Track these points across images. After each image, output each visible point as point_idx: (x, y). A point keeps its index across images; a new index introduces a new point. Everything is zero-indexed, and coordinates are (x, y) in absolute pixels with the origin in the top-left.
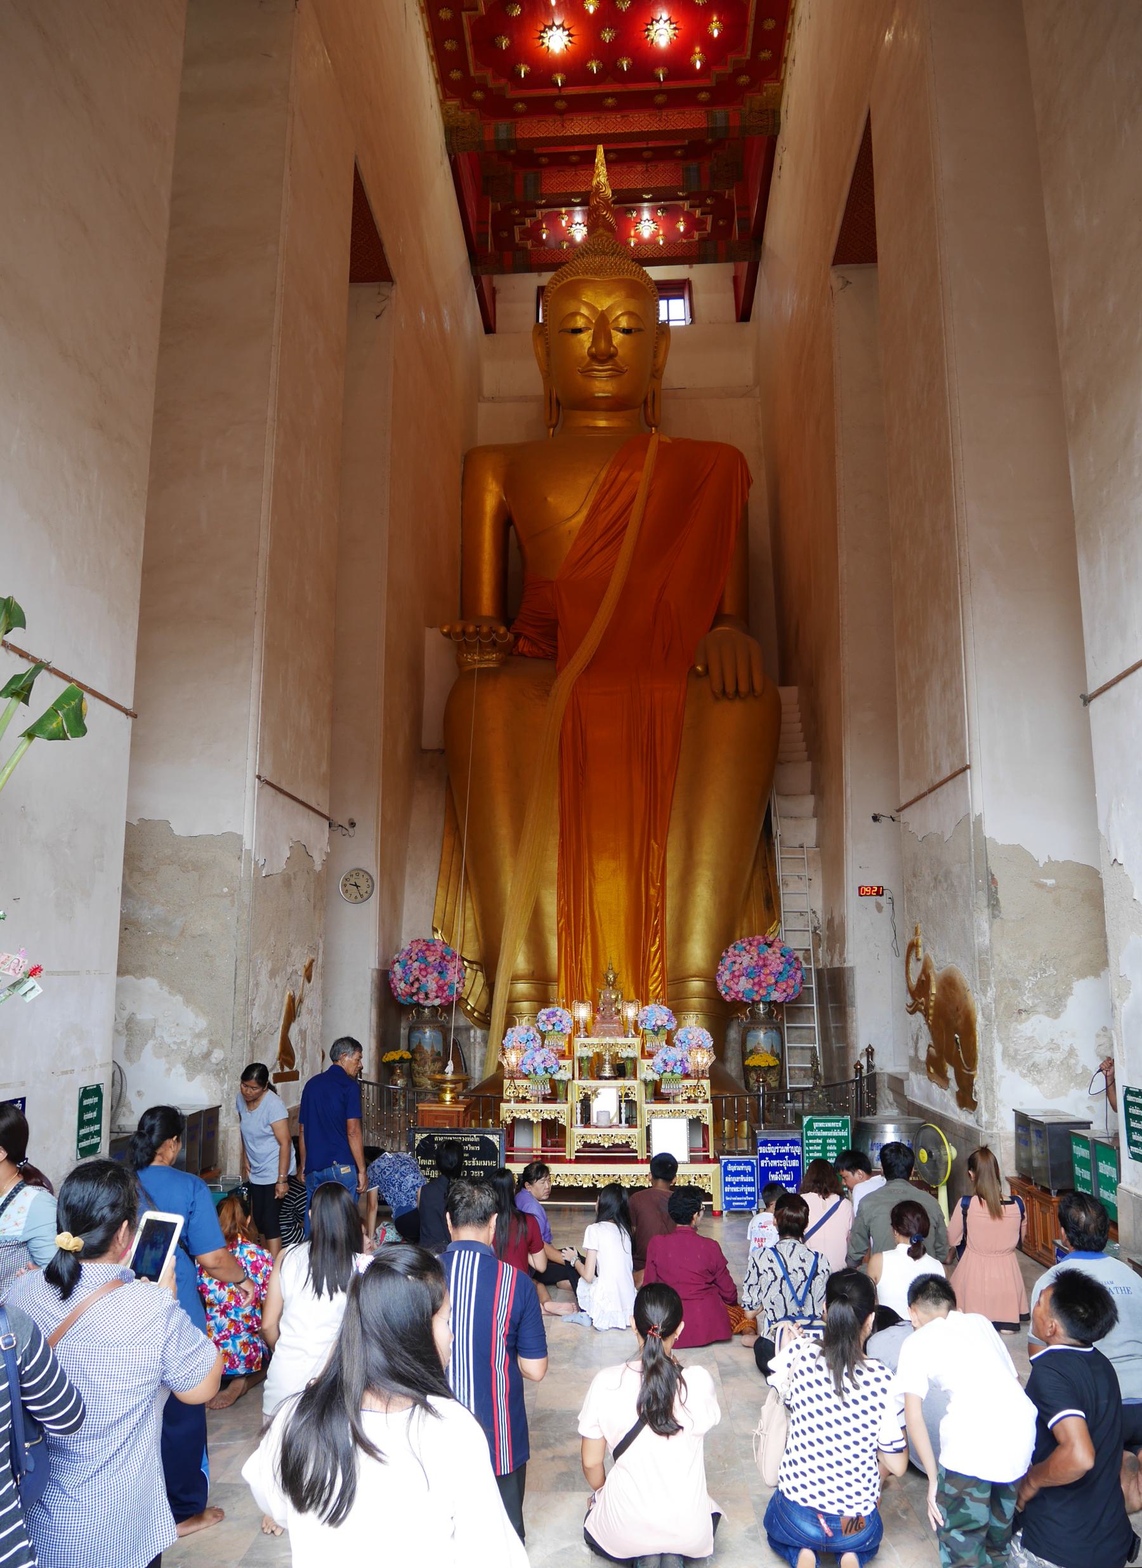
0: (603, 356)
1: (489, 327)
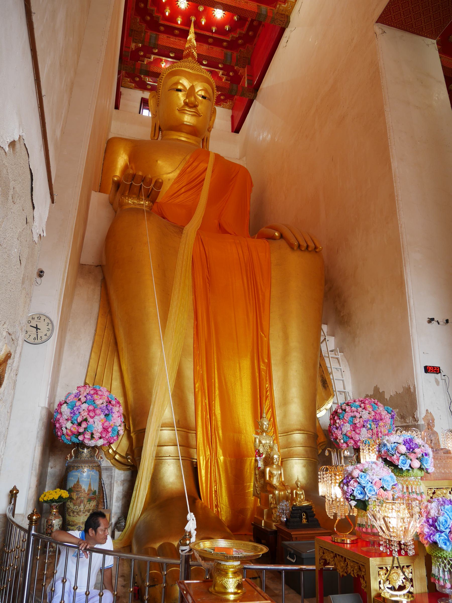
0: (191, 105)
1: (117, 107)
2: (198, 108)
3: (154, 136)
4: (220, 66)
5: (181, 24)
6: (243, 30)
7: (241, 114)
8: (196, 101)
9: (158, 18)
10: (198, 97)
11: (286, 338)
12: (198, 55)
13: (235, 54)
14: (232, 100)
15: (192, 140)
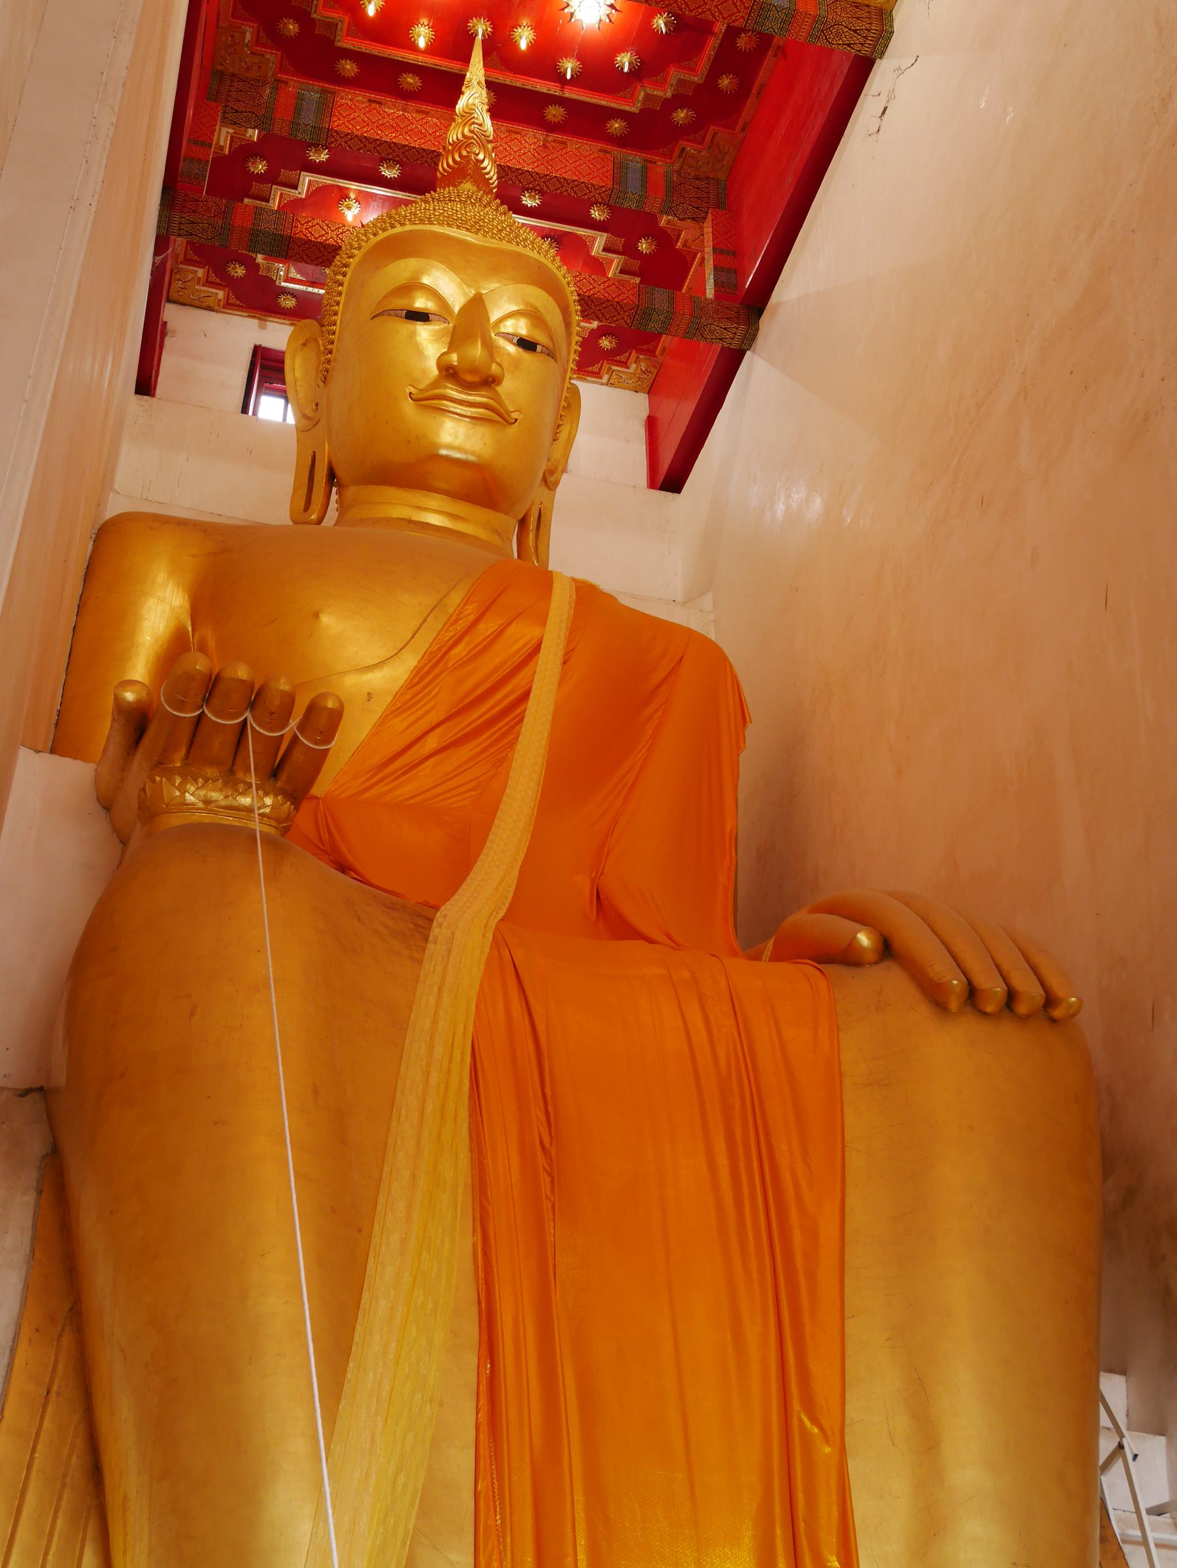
0: (470, 378)
1: (145, 385)
2: (500, 389)
3: (307, 508)
4: (596, 214)
5: (431, 50)
6: (693, 70)
7: (683, 412)
8: (493, 360)
9: (332, 26)
10: (502, 342)
11: (927, 1442)
12: (502, 170)
13: (662, 167)
14: (651, 353)
15: (474, 523)
